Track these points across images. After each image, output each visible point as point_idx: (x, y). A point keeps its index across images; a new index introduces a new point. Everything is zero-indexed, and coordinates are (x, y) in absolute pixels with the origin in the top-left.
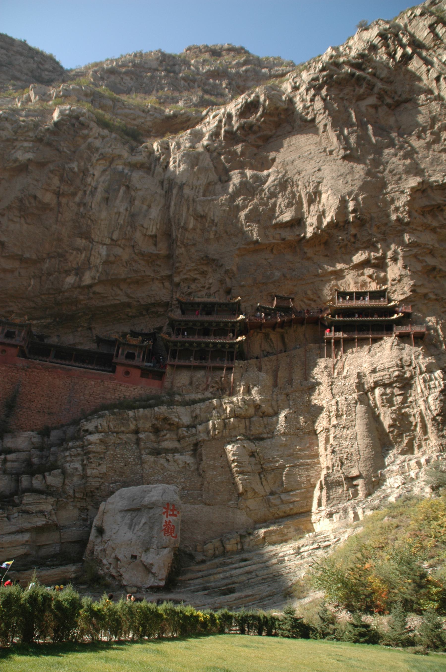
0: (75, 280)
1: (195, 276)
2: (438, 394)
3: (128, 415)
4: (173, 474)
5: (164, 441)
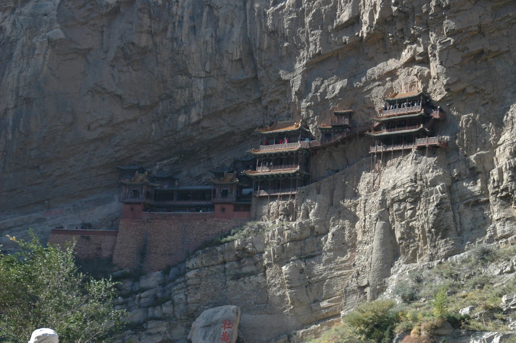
0: (186, 119)
1: (277, 98)
2: (433, 208)
3: (217, 250)
4: (248, 293)
5: (244, 267)
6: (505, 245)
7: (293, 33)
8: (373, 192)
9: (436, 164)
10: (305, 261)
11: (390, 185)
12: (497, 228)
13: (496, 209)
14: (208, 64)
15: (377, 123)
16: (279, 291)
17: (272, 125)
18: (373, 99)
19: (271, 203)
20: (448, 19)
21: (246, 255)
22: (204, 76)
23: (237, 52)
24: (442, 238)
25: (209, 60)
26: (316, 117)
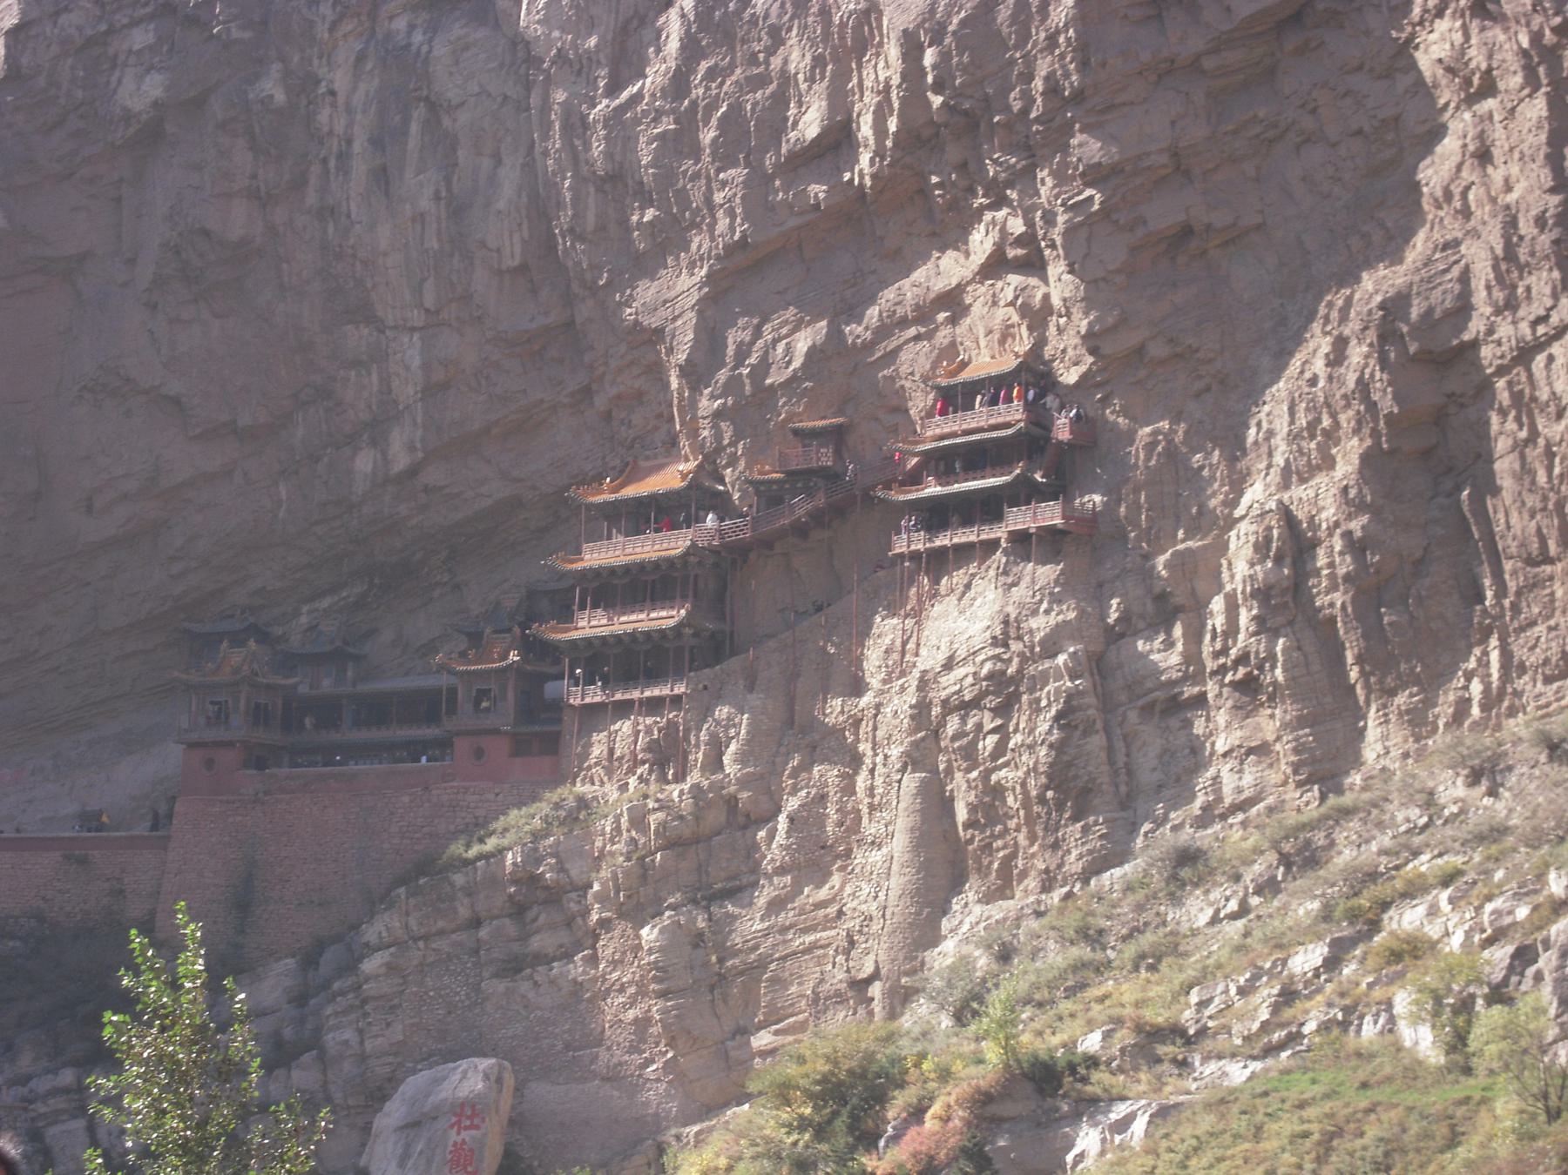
0: (375, 463)
1: (636, 386)
2: (1046, 726)
3: (452, 885)
6: (1240, 833)
7: (667, 176)
8: (898, 679)
9: (1062, 585)
10: (707, 908)
11: (941, 657)
12: (1224, 781)
13: (1221, 718)
14: (429, 285)
15: (916, 460)
16: (632, 1005)
17: (630, 473)
18: (903, 382)
19: (617, 726)
20: (1082, 131)
21: (541, 895)
22: (421, 325)
23: (512, 245)
24: (1075, 818)
25: (432, 272)
26: (740, 446)
